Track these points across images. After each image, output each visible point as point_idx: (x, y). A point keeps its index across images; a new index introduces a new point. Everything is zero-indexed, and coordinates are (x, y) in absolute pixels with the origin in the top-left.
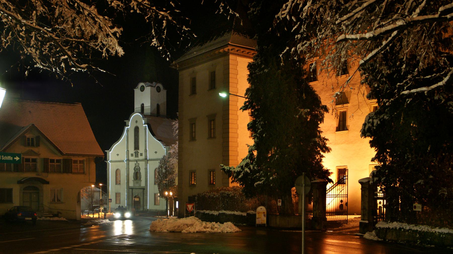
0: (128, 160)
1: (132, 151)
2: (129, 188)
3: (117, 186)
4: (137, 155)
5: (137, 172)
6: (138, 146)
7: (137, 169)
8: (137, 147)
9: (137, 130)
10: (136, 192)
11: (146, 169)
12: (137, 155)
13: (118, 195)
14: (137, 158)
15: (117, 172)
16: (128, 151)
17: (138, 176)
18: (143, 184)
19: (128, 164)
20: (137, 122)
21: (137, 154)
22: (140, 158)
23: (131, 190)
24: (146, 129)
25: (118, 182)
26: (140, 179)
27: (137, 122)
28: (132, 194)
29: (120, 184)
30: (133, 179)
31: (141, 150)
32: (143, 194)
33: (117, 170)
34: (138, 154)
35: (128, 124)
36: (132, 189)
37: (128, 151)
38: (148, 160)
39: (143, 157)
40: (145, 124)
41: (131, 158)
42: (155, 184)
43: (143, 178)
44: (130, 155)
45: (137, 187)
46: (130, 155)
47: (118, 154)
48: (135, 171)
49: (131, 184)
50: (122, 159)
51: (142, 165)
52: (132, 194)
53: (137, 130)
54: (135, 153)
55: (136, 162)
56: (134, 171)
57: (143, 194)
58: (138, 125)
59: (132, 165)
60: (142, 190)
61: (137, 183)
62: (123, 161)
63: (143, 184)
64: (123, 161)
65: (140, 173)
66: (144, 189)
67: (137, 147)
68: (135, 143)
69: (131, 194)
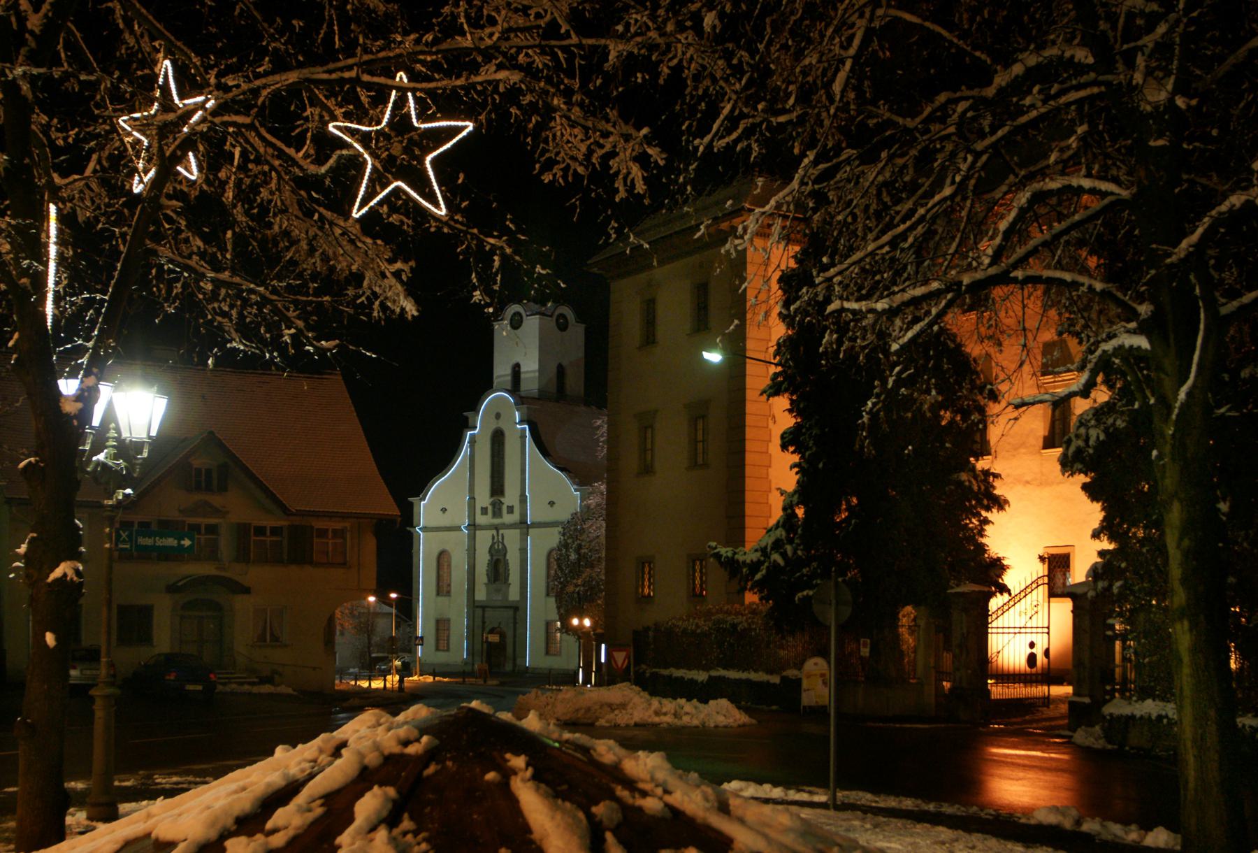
0: (473, 526)
1: (484, 499)
2: (473, 605)
3: (440, 599)
4: (497, 509)
5: (497, 561)
6: (502, 486)
7: (498, 551)
9: (498, 438)
11: (523, 551)
12: (497, 513)
13: (442, 625)
14: (497, 521)
15: (442, 559)
16: (472, 499)
17: (501, 570)
18: (514, 595)
19: (472, 538)
20: (498, 416)
21: (497, 509)
22: (507, 518)
23: (479, 612)
24: (523, 437)
25: (442, 588)
26: (507, 579)
27: (498, 416)
28: (484, 623)
29: (448, 593)
30: (485, 580)
31: (510, 497)
32: (515, 623)
34: (500, 509)
35: (475, 422)
36: (483, 608)
37: (472, 499)
38: (528, 527)
39: (515, 517)
40: (521, 422)
41: (481, 519)
42: (548, 595)
43: (514, 577)
44: (478, 511)
45: (498, 604)
46: (478, 511)
47: (443, 506)
48: (492, 555)
49: (481, 595)
50: (456, 523)
52: (484, 623)
53: (498, 438)
54: (493, 504)
55: (494, 532)
56: (488, 557)
57: (515, 623)
58: (502, 424)
59: (484, 540)
60: (511, 612)
61: (498, 591)
62: (458, 528)
63: (514, 595)
64: (458, 528)
66: (517, 610)
67: (497, 489)
68: (493, 477)
69: (478, 622)
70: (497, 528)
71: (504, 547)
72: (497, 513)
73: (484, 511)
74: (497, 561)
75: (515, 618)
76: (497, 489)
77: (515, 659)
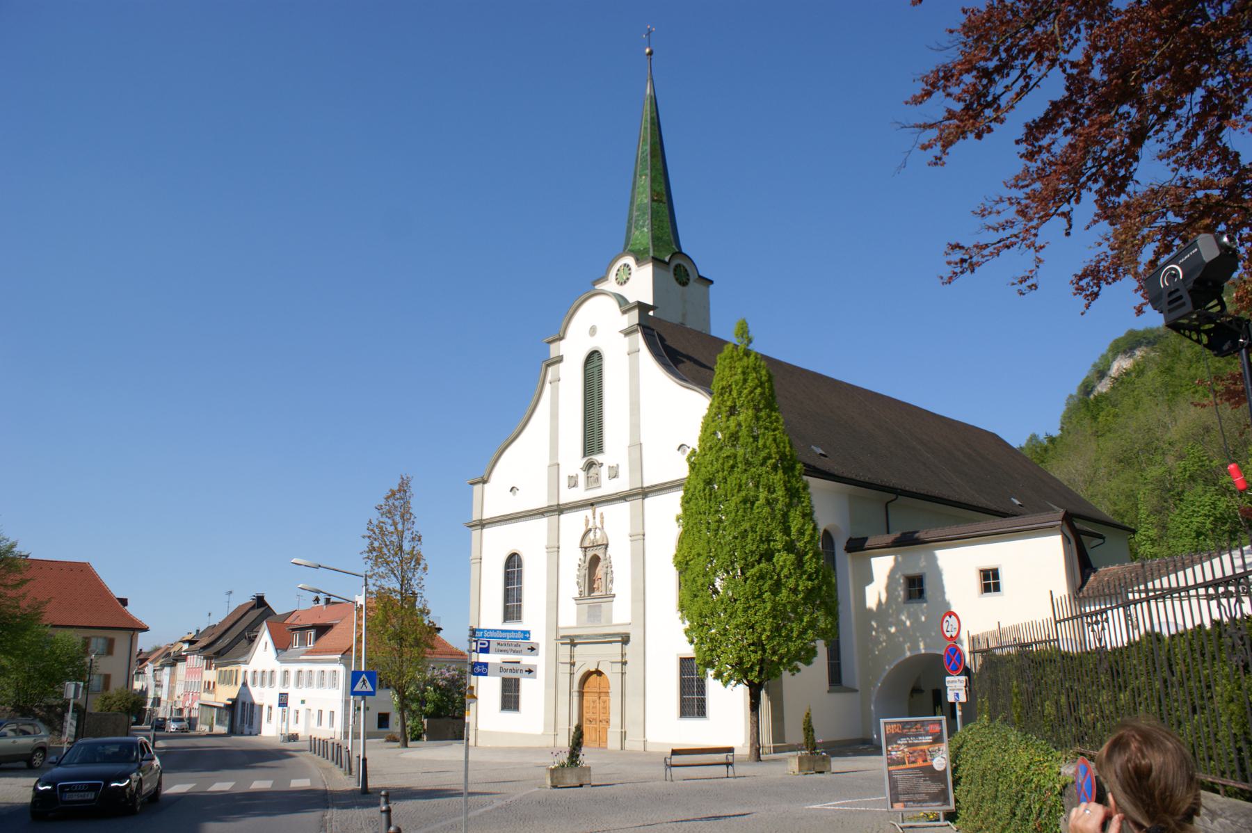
1: (572, 458)
8: (593, 440)
9: (593, 360)
10: (587, 658)
11: (639, 537)
12: (593, 482)
15: (513, 565)
18: (620, 614)
20: (593, 331)
22: (608, 487)
27: (593, 331)
36: (573, 642)
49: (570, 617)
53: (593, 360)
56: (580, 554)
63: (620, 614)
65: (609, 566)
67: (593, 440)
70: (592, 504)
71: (605, 536)
72: (593, 482)
74: (595, 561)
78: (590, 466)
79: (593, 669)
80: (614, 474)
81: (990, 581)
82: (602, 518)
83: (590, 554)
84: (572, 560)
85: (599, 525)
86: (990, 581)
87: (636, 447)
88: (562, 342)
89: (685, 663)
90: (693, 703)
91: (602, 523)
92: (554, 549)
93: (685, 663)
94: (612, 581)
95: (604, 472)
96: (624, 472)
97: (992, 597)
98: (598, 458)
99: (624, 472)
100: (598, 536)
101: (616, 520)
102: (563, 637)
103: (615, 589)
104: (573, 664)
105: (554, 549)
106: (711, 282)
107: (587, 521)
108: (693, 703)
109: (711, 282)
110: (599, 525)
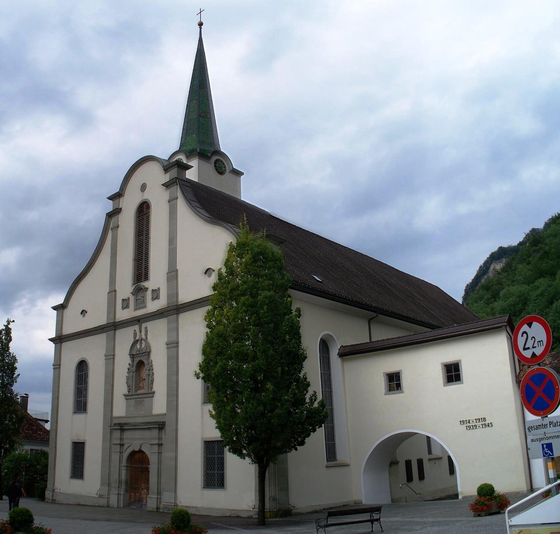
1: (125, 287)
9: (143, 210)
10: (135, 441)
11: (173, 346)
12: (140, 304)
13: (78, 449)
16: (113, 292)
18: (159, 405)
22: (152, 306)
30: (125, 390)
31: (157, 278)
33: (82, 366)
37: (113, 292)
39: (162, 303)
43: (160, 385)
48: (132, 356)
49: (120, 409)
51: (157, 335)
53: (143, 210)
56: (128, 360)
58: (147, 196)
63: (159, 405)
65: (151, 369)
70: (138, 321)
73: (126, 304)
74: (141, 364)
75: (160, 439)
76: (141, 271)
77: (159, 493)
78: (139, 291)
79: (137, 449)
80: (156, 294)
81: (453, 373)
82: (146, 331)
83: (137, 360)
84: (123, 362)
85: (143, 337)
86: (453, 373)
87: (173, 275)
88: (121, 199)
89: (209, 445)
90: (214, 477)
91: (146, 335)
92: (110, 357)
93: (209, 445)
94: (152, 381)
95: (149, 294)
96: (163, 294)
97: (454, 387)
98: (145, 284)
99: (163, 294)
100: (143, 346)
101: (157, 335)
102: (115, 424)
103: (155, 388)
104: (122, 445)
105: (110, 357)
106: (243, 174)
107: (135, 334)
108: (214, 477)
109: (243, 174)
110: (143, 337)
